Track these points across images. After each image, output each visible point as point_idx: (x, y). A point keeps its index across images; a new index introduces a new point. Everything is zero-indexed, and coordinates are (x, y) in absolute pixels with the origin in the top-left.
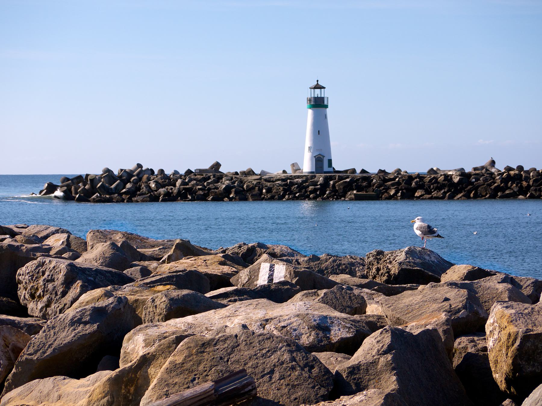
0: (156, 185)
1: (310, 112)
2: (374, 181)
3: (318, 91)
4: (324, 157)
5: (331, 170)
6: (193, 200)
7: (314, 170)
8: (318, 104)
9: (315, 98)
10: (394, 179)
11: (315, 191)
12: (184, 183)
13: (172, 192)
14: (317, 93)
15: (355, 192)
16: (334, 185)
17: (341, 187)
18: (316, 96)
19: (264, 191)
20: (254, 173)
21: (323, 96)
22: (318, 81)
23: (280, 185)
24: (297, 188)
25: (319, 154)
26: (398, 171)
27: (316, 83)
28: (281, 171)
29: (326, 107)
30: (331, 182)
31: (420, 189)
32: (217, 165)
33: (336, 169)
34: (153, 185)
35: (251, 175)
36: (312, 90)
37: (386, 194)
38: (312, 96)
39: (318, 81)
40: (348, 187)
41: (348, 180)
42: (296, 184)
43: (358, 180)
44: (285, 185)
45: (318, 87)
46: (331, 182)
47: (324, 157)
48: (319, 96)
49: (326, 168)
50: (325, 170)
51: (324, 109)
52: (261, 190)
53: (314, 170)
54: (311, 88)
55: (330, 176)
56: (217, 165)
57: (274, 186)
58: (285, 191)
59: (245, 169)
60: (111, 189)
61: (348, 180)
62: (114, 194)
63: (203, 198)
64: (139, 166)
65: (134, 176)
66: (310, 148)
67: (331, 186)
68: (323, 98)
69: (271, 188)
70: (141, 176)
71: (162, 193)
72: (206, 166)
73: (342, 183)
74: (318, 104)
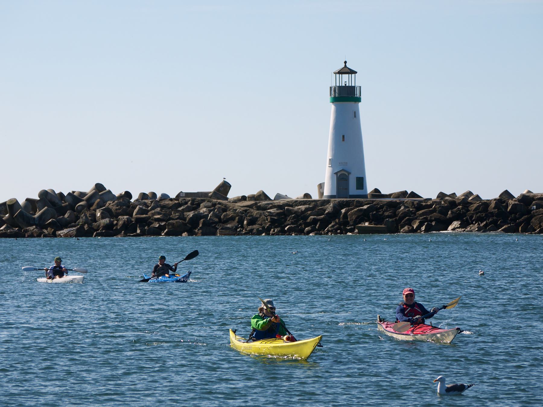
0: (101, 214)
1: (332, 108)
2: (402, 208)
3: (345, 77)
4: (349, 173)
5: (360, 192)
6: (143, 234)
7: (335, 194)
8: (346, 97)
9: (339, 87)
10: (431, 206)
11: (315, 221)
12: (141, 211)
13: (117, 224)
14: (345, 79)
15: (367, 224)
16: (346, 213)
17: (354, 217)
18: (344, 85)
19: (245, 222)
20: (266, 197)
21: (353, 85)
22: (345, 62)
23: (271, 214)
24: (294, 218)
25: (343, 170)
26: (442, 195)
27: (343, 65)
28: (302, 195)
29: (358, 100)
30: (343, 211)
31: (457, 220)
32: (225, 187)
33: (383, 193)
34: (98, 214)
35: (262, 200)
36: (338, 75)
37: (406, 228)
38: (338, 85)
39: (345, 62)
40: (363, 216)
41: (365, 207)
42: (296, 212)
43: (382, 207)
44: (278, 214)
45: (346, 71)
46: (343, 211)
47: (349, 173)
48: (347, 85)
49: (353, 190)
50: (351, 193)
51: (352, 103)
52: (241, 222)
53: (335, 194)
54: (334, 73)
55: (347, 202)
56: (225, 187)
57: (261, 215)
58: (273, 222)
59: (255, 192)
60: (34, 218)
61: (365, 207)
62: (32, 225)
63: (157, 232)
64: (99, 187)
65: (83, 201)
66: (332, 162)
67: (342, 216)
68: (355, 87)
69: (257, 218)
70: (92, 201)
71: (102, 225)
72: (209, 186)
73: (356, 211)
74: (346, 97)
